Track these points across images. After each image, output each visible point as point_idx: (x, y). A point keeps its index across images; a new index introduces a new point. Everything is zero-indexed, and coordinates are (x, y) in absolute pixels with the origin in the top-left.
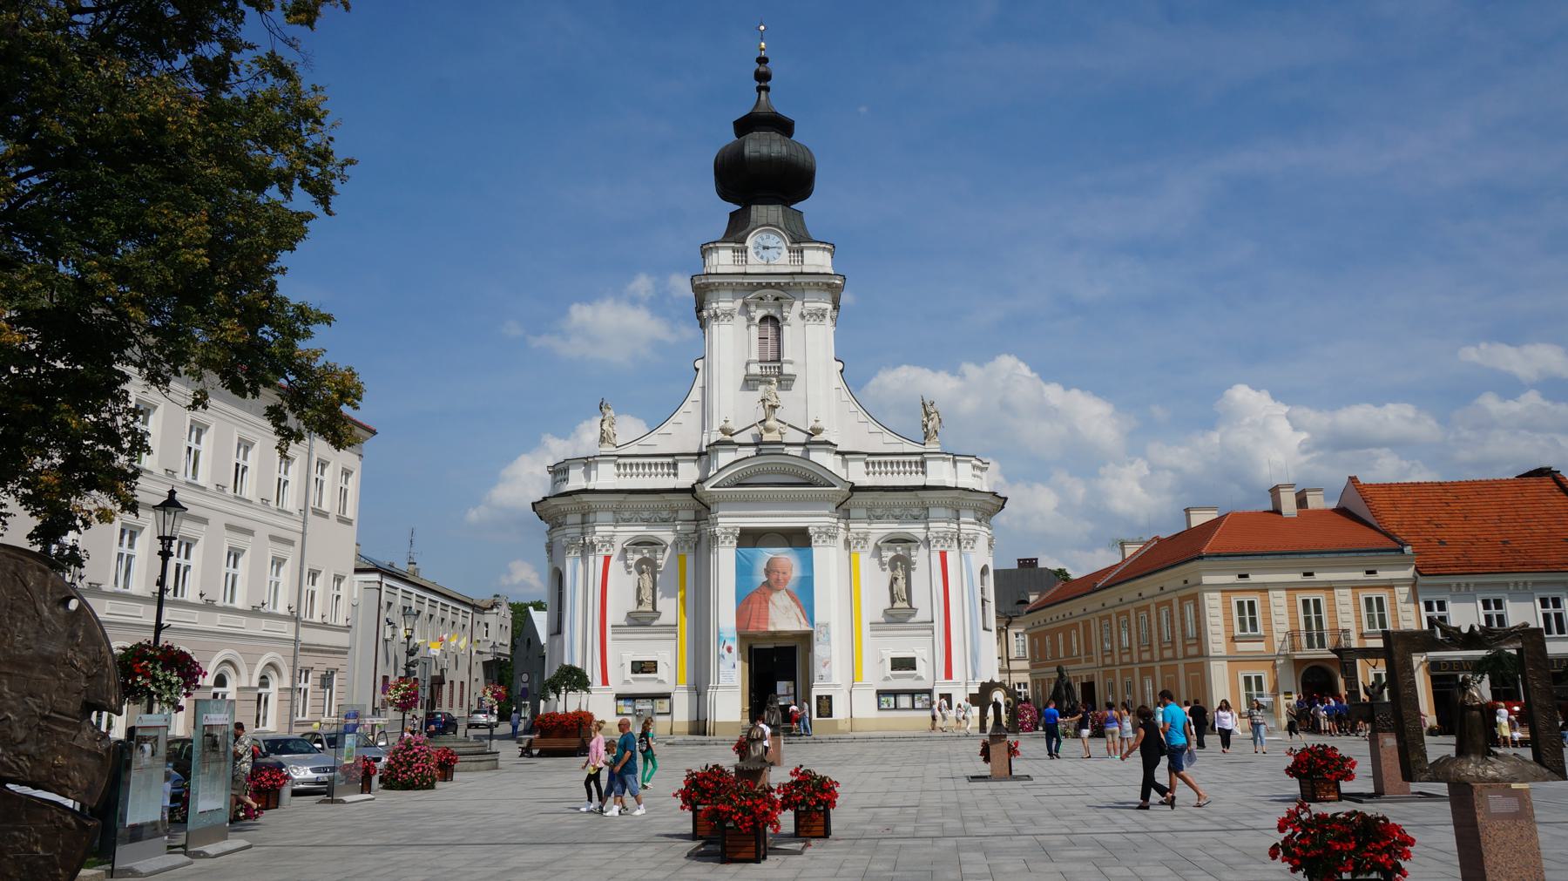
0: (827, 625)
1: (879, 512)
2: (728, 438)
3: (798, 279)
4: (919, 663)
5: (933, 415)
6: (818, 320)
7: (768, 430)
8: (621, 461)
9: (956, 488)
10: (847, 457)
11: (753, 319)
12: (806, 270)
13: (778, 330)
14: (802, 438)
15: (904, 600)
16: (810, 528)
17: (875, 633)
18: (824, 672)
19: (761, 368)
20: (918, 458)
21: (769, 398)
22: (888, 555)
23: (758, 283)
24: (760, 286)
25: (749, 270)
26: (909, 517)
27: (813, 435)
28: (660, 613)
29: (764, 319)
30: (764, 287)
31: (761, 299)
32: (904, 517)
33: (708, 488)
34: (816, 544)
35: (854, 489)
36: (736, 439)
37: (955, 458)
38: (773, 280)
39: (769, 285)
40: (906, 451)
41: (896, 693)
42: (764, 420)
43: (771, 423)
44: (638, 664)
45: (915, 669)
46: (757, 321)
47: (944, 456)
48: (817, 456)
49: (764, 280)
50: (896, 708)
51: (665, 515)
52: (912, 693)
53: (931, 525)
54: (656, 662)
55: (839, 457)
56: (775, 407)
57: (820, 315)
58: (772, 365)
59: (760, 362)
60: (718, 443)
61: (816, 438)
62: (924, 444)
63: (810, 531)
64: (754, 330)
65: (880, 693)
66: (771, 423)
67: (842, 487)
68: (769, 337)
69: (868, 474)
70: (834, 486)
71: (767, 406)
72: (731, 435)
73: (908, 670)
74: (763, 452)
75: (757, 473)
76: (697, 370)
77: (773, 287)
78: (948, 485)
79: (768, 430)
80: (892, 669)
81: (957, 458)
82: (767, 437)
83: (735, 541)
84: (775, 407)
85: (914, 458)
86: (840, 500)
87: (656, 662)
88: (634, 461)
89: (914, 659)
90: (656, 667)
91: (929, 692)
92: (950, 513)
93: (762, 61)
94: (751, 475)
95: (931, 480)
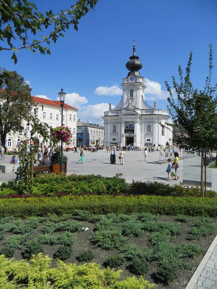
0: (136, 135)
1: (146, 118)
3: (136, 83)
7: (129, 107)
8: (112, 112)
9: (158, 115)
12: (137, 82)
13: (133, 91)
14: (133, 108)
18: (135, 141)
20: (153, 110)
22: (147, 124)
24: (130, 85)
25: (129, 83)
29: (131, 90)
37: (158, 110)
38: (132, 84)
39: (131, 85)
41: (147, 144)
43: (130, 106)
49: (131, 84)
51: (117, 119)
52: (150, 144)
53: (154, 120)
55: (141, 110)
61: (136, 108)
64: (129, 92)
66: (130, 106)
75: (127, 113)
79: (129, 107)
82: (129, 108)
86: (139, 117)
91: (152, 144)
93: (134, 46)
95: (154, 113)
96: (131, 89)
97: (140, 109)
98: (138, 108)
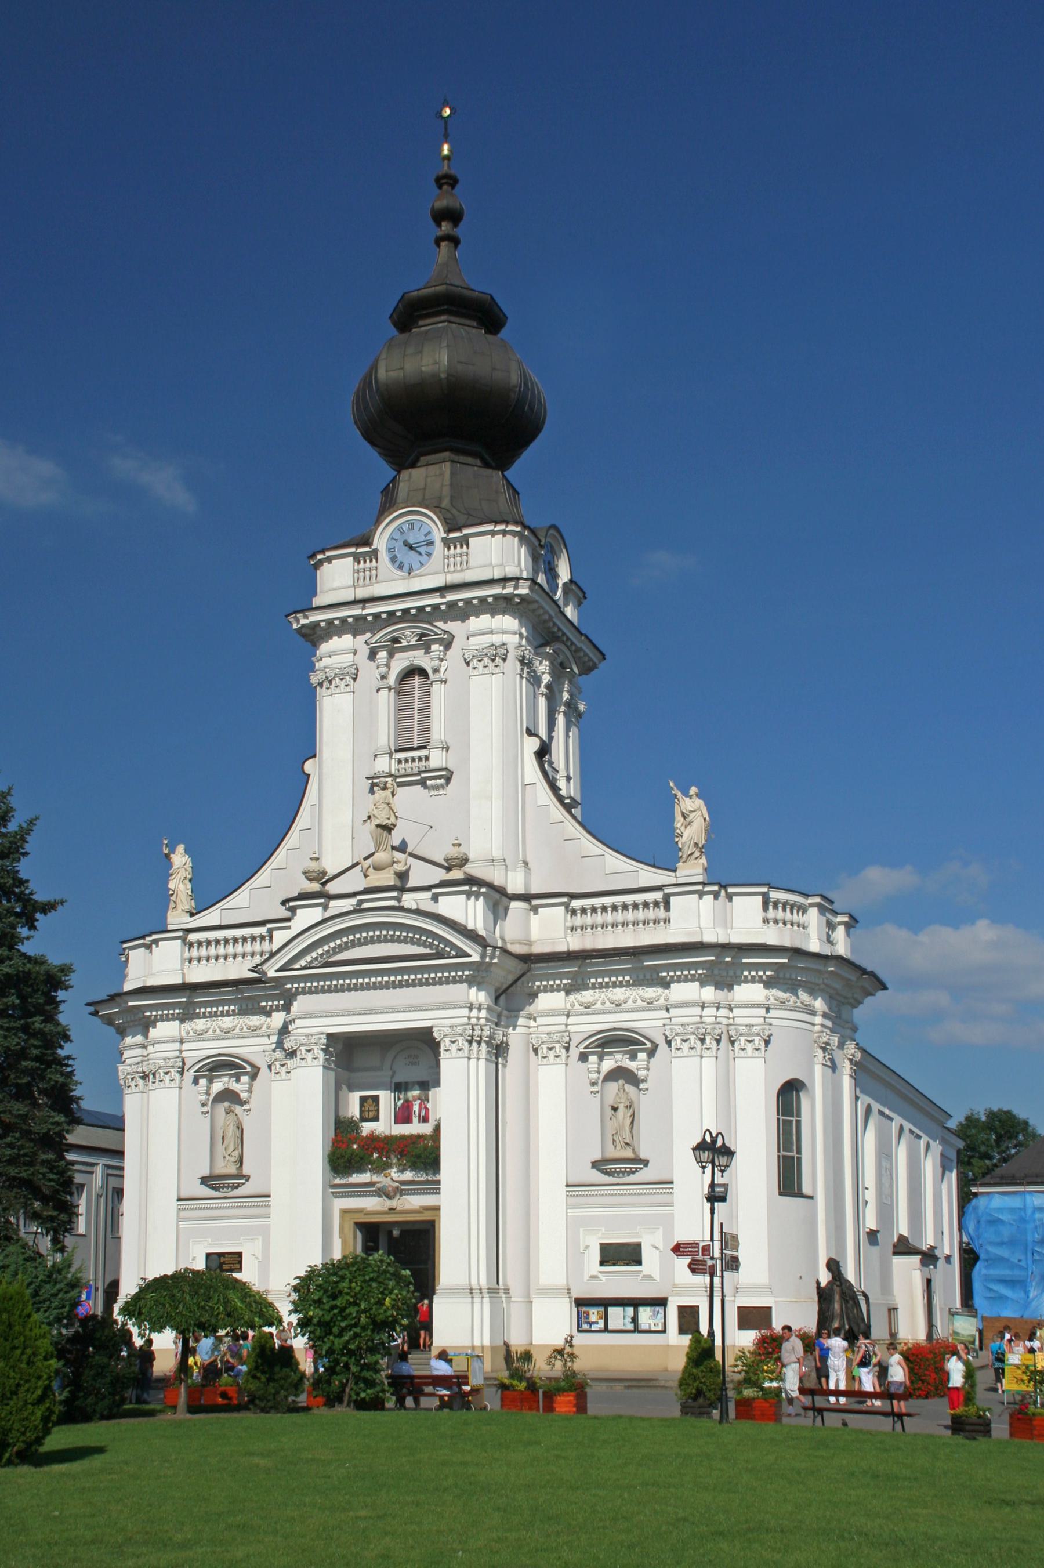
2: (315, 887)
4: (647, 1254)
5: (692, 815)
6: (491, 665)
10: (535, 902)
11: (383, 677)
15: (627, 1144)
16: (435, 1029)
17: (572, 1200)
19: (399, 761)
20: (658, 896)
21: (375, 812)
23: (391, 614)
26: (639, 1001)
27: (449, 869)
28: (247, 1178)
30: (401, 620)
31: (395, 640)
32: (630, 1002)
33: (271, 973)
34: (447, 1054)
35: (527, 959)
36: (332, 888)
40: (642, 885)
42: (372, 855)
44: (216, 1257)
45: (639, 1263)
46: (392, 680)
47: (700, 887)
48: (453, 906)
50: (606, 1330)
52: (636, 1303)
54: (240, 1255)
56: (388, 829)
57: (497, 655)
58: (416, 754)
59: (397, 751)
60: (303, 896)
61: (456, 874)
62: (674, 871)
63: (435, 1035)
64: (385, 700)
65: (580, 1303)
67: (483, 956)
68: (416, 707)
69: (572, 929)
70: (469, 956)
71: (373, 826)
72: (324, 884)
73: (627, 1265)
74: (366, 905)
76: (309, 776)
77: (415, 619)
78: (709, 938)
79: (377, 868)
80: (602, 1263)
81: (730, 890)
83: (321, 1055)
84: (388, 829)
85: (650, 897)
87: (240, 1255)
88: (212, 935)
89: (638, 1246)
90: (240, 1262)
92: (709, 993)
94: (346, 947)
96: (407, 663)
97: (510, 890)
98: (471, 880)
